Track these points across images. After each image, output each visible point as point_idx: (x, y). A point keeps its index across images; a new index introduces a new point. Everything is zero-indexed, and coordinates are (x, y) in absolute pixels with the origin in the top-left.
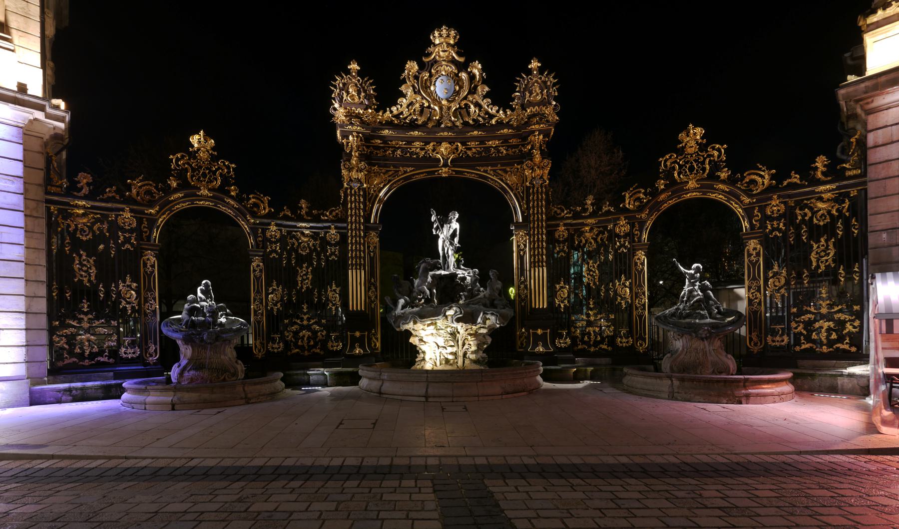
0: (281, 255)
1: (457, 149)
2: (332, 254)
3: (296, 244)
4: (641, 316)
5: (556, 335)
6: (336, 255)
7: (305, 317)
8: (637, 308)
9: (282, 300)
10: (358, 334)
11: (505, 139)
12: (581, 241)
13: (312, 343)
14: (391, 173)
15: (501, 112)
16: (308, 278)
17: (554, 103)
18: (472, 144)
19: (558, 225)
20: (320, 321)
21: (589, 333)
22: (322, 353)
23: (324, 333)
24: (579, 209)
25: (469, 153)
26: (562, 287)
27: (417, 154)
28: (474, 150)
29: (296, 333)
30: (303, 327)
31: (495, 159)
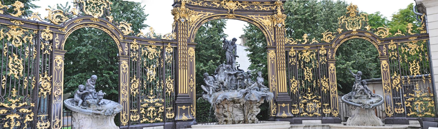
0: (138, 59)
1: (237, 5)
3: (147, 53)
4: (334, 97)
5: (292, 107)
8: (332, 93)
9: (138, 88)
10: (184, 107)
12: (302, 57)
13: (155, 115)
14: (200, 15)
23: (163, 108)
24: (300, 40)
25: (244, 7)
26: (294, 81)
28: (246, 6)
29: (146, 108)
30: (150, 105)
31: (256, 11)
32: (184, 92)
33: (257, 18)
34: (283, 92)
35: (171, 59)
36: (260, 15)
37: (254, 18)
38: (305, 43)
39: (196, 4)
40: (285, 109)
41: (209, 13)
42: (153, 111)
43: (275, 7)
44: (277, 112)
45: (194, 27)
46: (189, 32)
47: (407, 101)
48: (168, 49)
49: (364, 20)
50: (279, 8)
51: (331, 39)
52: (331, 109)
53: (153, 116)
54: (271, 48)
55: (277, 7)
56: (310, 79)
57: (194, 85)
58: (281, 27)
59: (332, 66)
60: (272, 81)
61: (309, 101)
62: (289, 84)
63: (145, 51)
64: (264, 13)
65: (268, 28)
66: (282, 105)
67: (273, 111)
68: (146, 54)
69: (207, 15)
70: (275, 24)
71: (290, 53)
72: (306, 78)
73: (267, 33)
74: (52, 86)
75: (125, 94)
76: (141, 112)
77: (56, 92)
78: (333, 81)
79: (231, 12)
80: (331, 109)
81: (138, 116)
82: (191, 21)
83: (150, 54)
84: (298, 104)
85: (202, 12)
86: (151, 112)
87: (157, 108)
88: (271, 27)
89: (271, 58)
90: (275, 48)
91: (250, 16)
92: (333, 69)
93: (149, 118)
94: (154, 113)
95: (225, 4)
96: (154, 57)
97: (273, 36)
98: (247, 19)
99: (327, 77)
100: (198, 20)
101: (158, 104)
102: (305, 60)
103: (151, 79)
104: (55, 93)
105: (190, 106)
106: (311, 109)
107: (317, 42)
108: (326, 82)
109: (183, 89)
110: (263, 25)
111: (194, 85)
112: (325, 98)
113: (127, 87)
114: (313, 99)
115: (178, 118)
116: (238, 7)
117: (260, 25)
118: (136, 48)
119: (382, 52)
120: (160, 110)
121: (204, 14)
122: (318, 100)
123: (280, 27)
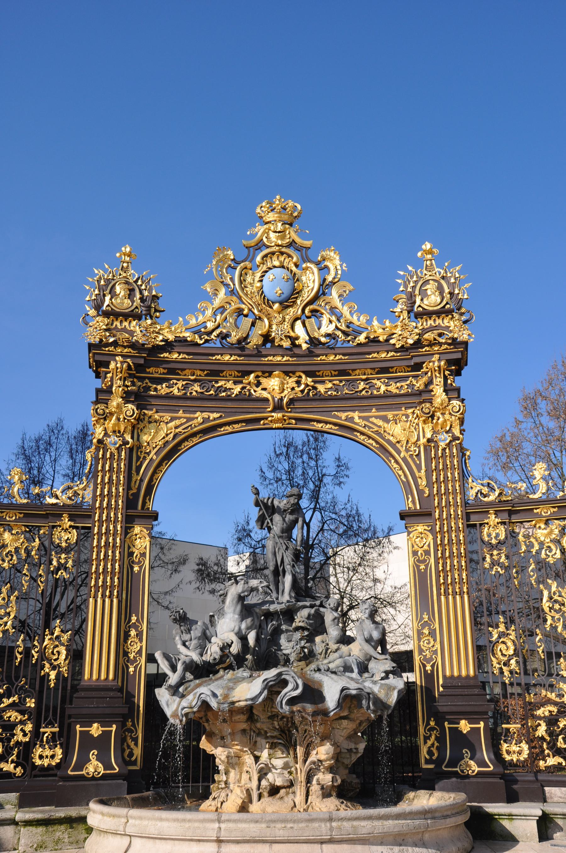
2: (62, 566)
6: (66, 569)
10: (95, 730)
14: (178, 422)
15: (375, 323)
16: (8, 614)
20: (22, 701)
22: (19, 771)
23: (29, 727)
25: (321, 388)
27: (226, 390)
28: (330, 385)
32: (103, 677)
33: (366, 419)
35: (70, 564)
37: (357, 420)
41: (205, 415)
43: (425, 379)
48: (63, 534)
50: (439, 381)
58: (448, 445)
64: (389, 402)
65: (407, 450)
69: (200, 420)
70: (429, 435)
71: (486, 530)
72: (549, 622)
73: (401, 469)
79: (278, 407)
88: (415, 443)
90: (429, 514)
91: (343, 415)
95: (258, 384)
98: (335, 424)
100: (166, 439)
101: (14, 716)
102: (543, 556)
109: (98, 668)
110: (389, 442)
111: (140, 652)
116: (302, 391)
117: (377, 442)
120: (19, 737)
121: (189, 420)
123: (442, 445)
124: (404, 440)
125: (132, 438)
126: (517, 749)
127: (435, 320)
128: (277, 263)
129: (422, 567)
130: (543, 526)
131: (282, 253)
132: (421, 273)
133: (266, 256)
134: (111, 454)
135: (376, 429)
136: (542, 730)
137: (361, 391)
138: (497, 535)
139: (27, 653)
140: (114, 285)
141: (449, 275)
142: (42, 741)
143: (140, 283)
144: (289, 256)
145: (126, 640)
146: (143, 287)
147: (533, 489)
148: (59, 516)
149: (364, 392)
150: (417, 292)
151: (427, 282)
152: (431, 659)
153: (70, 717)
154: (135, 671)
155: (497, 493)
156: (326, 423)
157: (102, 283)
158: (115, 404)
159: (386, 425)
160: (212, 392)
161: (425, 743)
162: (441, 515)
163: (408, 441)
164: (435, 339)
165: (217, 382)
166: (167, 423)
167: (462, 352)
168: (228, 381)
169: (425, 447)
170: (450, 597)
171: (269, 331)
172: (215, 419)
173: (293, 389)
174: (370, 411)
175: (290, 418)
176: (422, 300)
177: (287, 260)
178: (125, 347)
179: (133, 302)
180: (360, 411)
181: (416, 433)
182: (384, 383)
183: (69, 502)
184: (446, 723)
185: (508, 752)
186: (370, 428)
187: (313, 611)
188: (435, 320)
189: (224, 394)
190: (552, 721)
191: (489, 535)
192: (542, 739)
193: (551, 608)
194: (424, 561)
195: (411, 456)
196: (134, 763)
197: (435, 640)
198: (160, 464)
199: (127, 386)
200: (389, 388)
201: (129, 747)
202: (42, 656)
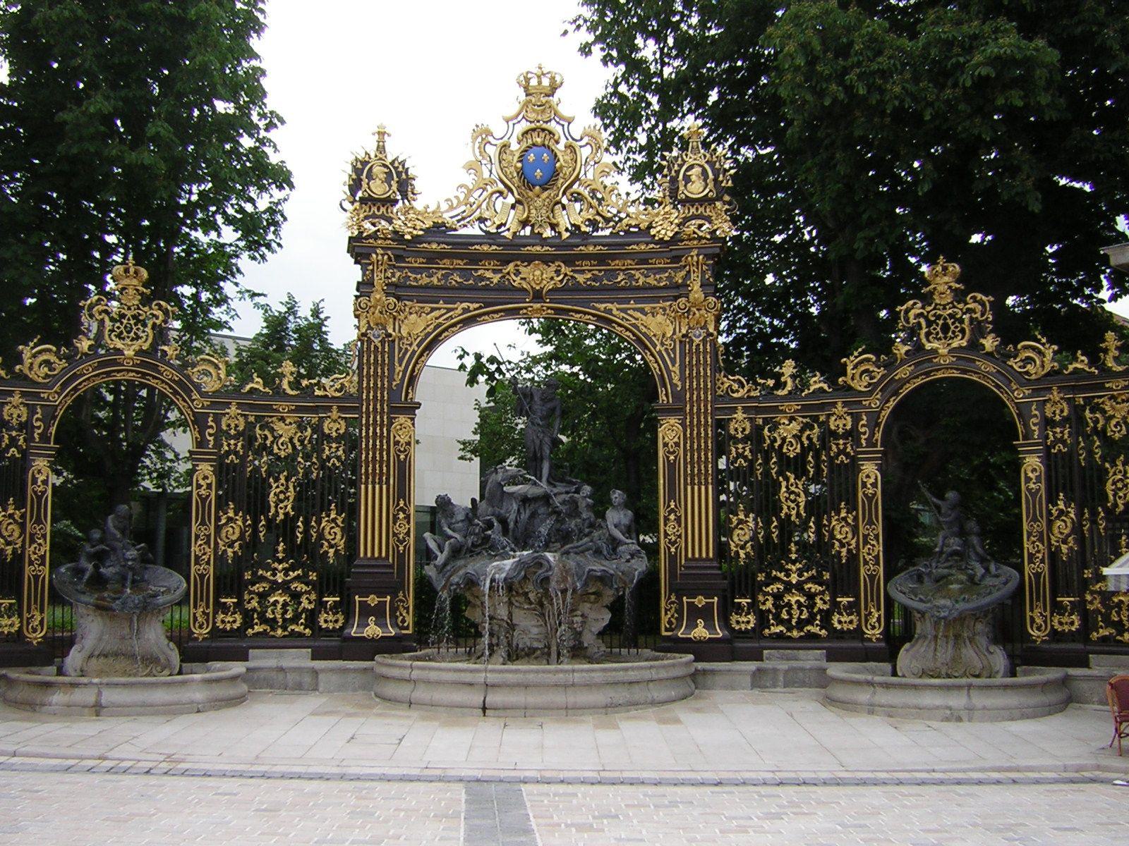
3: (270, 439)
5: (728, 607)
7: (280, 567)
10: (373, 600)
11: (643, 259)
12: (775, 440)
14: (436, 313)
16: (287, 498)
17: (727, 198)
18: (586, 265)
19: (734, 410)
20: (306, 575)
21: (789, 605)
23: (313, 597)
24: (771, 382)
25: (581, 278)
28: (589, 276)
30: (275, 586)
31: (623, 289)
32: (376, 555)
34: (700, 559)
36: (637, 301)
37: (615, 312)
38: (785, 392)
39: (424, 280)
40: (705, 614)
41: (465, 305)
42: (285, 605)
43: (683, 273)
44: (680, 620)
45: (414, 352)
46: (398, 369)
47: (1092, 593)
49: (978, 315)
51: (872, 378)
52: (859, 614)
53: (285, 620)
54: (670, 411)
55: (689, 272)
56: (798, 515)
57: (408, 534)
58: (704, 341)
59: (870, 471)
60: (666, 519)
61: (789, 587)
62: (723, 528)
63: (266, 432)
64: (648, 294)
65: (662, 344)
66: (696, 601)
67: (664, 620)
68: (268, 443)
69: (459, 311)
70: (684, 331)
71: (732, 425)
72: (785, 510)
74: (23, 532)
75: (205, 554)
76: (249, 607)
77: (32, 549)
78: (870, 523)
80: (859, 614)
81: (238, 617)
82: (405, 334)
83: (281, 441)
84: (754, 598)
85: (441, 304)
86: (279, 606)
87: (296, 596)
89: (666, 445)
91: (602, 306)
92: (872, 480)
93: (272, 623)
94: (285, 612)
95: (517, 273)
96: (290, 450)
97: (676, 369)
99: (852, 507)
100: (428, 330)
102: (785, 450)
103: (281, 511)
104: (32, 549)
105: (394, 596)
106: (796, 613)
107: (825, 386)
108: (848, 524)
110: (644, 334)
112: (843, 577)
113: (208, 536)
114: (806, 582)
115: (353, 632)
116: (561, 281)
117: (634, 334)
118: (237, 426)
119: (1026, 425)
121: (449, 310)
122: (820, 585)
124: (659, 333)
125: (394, 330)
126: (745, 620)
127: (697, 209)
128: (539, 140)
129: (672, 457)
130: (787, 422)
131: (543, 130)
132: (686, 155)
133: (526, 132)
134: (376, 347)
135: (634, 321)
136: (769, 605)
137: (620, 282)
138: (744, 429)
139: (306, 532)
140: (371, 168)
141: (715, 159)
142: (326, 608)
143: (396, 164)
144: (550, 133)
145: (395, 523)
146: (400, 169)
147: (780, 385)
148: (329, 409)
149: (623, 283)
150: (681, 177)
151: (691, 167)
152: (675, 542)
153: (349, 589)
154: (404, 551)
155: (746, 390)
156: (585, 313)
157: (359, 166)
158: (378, 297)
159: (644, 318)
160: (471, 282)
161: (666, 614)
162: (691, 409)
163: (664, 335)
164: (694, 233)
165: (476, 270)
166: (427, 314)
167: (720, 247)
168: (488, 270)
169: (681, 342)
170: (696, 487)
171: (528, 217)
172: (475, 309)
173: (552, 278)
174: (629, 303)
175: (548, 308)
176: (685, 186)
177: (548, 137)
178: (386, 239)
179: (390, 186)
180: (621, 301)
181: (671, 328)
182: (642, 274)
183: (338, 394)
184: (685, 598)
185: (738, 622)
186: (627, 320)
187: (567, 497)
188: (697, 209)
189: (483, 283)
190: (778, 597)
191: (736, 430)
192: (769, 611)
193: (787, 499)
194: (674, 452)
195: (666, 350)
196: (407, 628)
197: (680, 526)
198: (421, 355)
199: (388, 278)
200: (648, 280)
201: (401, 615)
202: (321, 536)
